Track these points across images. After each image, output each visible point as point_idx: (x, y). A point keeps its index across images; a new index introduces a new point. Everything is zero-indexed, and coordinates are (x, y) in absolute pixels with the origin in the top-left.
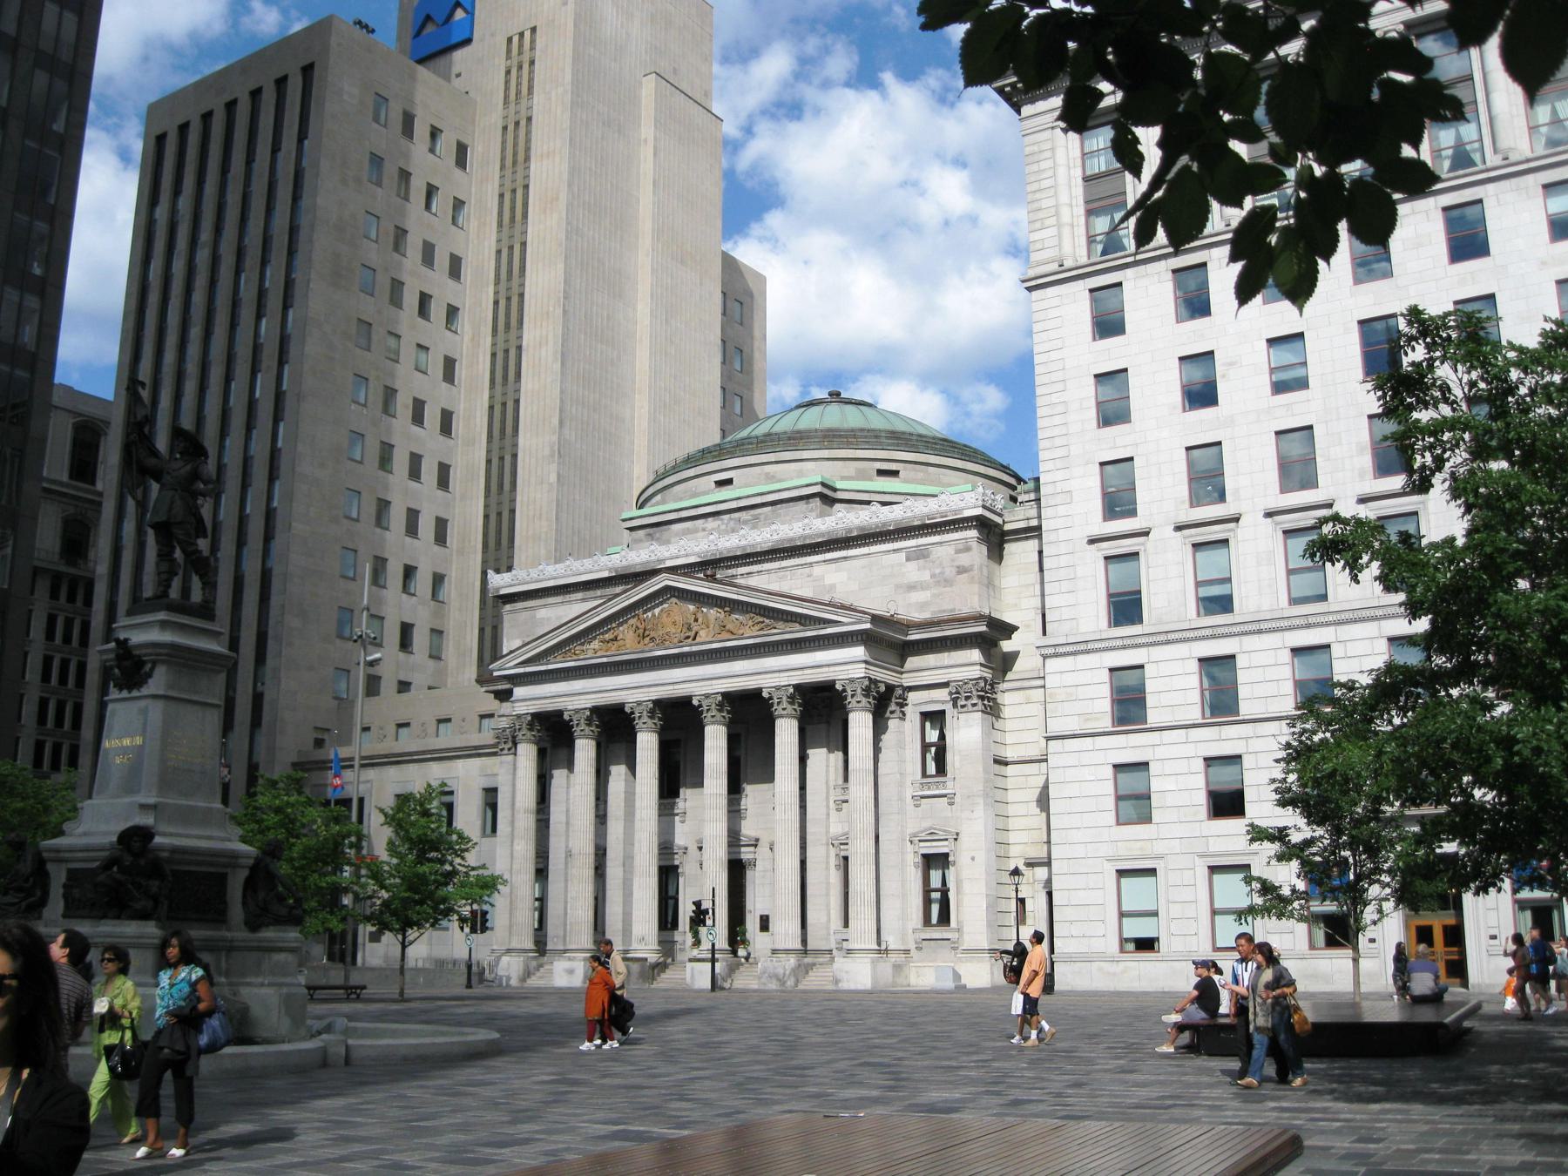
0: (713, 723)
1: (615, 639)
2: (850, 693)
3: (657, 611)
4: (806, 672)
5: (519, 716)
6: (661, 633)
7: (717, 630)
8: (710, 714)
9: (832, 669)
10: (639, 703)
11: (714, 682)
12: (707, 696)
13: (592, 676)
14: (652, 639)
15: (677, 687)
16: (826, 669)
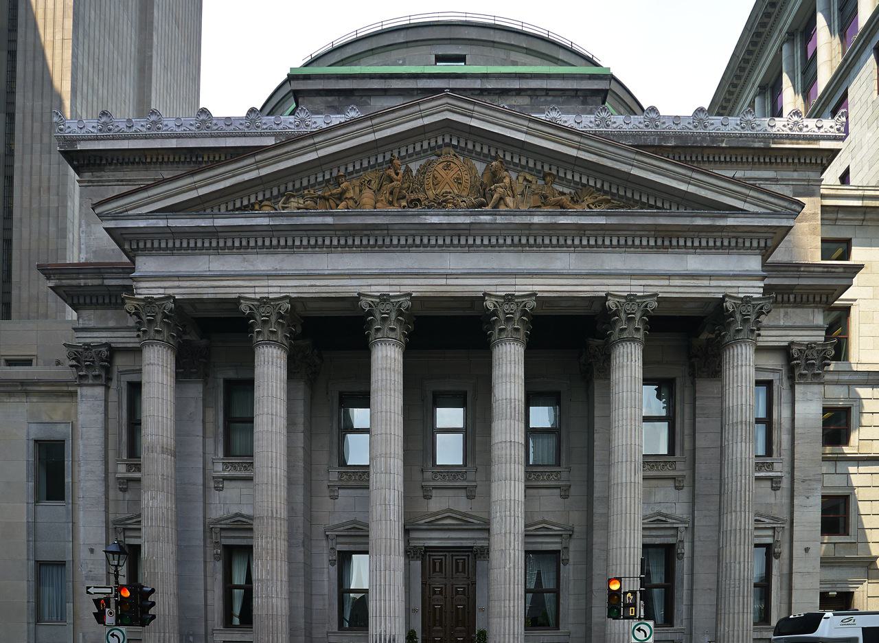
0: (516, 340)
1: (340, 197)
2: (738, 317)
3: (414, 167)
4: (673, 282)
5: (149, 301)
6: (431, 194)
7: (534, 200)
8: (509, 328)
9: (713, 283)
10: (384, 298)
11: (518, 281)
12: (509, 298)
13: (291, 249)
14: (415, 203)
15: (450, 282)
16: (706, 283)
